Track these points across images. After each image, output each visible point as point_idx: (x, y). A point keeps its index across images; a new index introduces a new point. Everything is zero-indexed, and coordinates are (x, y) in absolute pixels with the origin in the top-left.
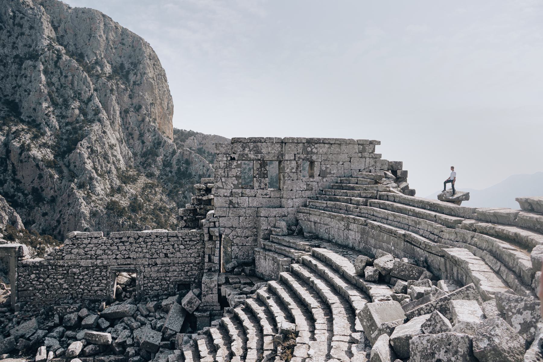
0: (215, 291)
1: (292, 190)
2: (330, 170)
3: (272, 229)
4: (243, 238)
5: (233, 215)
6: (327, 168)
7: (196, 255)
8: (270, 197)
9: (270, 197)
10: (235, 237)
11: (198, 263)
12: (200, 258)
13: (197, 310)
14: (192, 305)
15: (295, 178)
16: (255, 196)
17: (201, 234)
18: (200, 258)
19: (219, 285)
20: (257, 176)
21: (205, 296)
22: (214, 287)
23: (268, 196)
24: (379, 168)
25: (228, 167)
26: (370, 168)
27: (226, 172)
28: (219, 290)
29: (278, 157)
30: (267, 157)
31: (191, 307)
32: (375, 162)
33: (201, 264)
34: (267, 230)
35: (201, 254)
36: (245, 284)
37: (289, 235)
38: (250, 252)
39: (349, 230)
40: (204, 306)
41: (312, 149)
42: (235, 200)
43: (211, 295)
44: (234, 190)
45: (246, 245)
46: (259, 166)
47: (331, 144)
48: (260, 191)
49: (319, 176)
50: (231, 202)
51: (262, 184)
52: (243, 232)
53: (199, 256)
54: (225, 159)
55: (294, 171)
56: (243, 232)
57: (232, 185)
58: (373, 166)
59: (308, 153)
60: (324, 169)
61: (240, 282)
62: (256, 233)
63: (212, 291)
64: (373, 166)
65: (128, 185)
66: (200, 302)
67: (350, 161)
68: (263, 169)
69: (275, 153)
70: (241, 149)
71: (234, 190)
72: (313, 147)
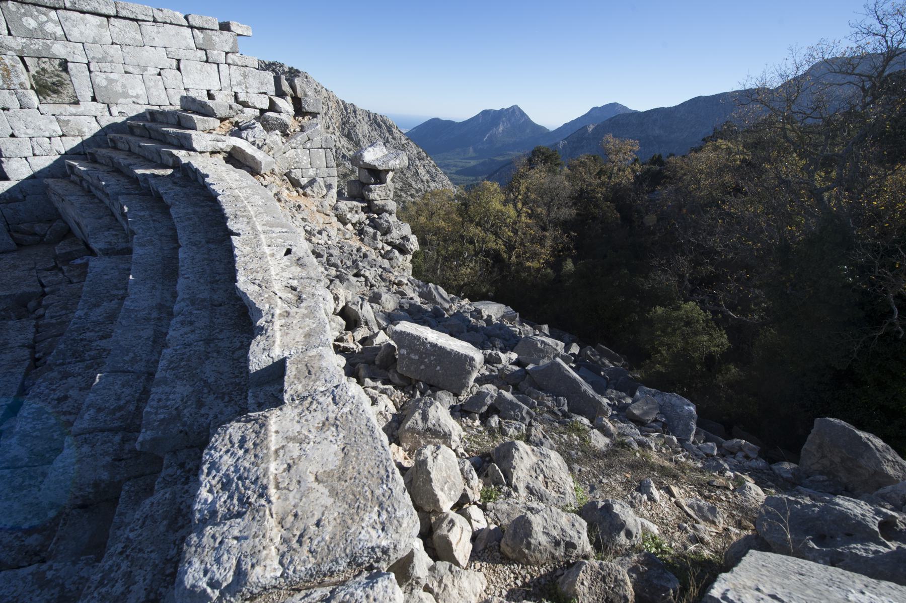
1: (12, 136)
2: (124, 86)
6: (110, 81)
24: (257, 91)
26: (235, 89)
32: (245, 76)
41: (41, 25)
47: (108, 17)
49: (94, 99)
58: (239, 84)
59: (31, 35)
60: (104, 83)
64: (239, 84)
65: (48, 98)
67: (179, 69)
72: (44, 18)
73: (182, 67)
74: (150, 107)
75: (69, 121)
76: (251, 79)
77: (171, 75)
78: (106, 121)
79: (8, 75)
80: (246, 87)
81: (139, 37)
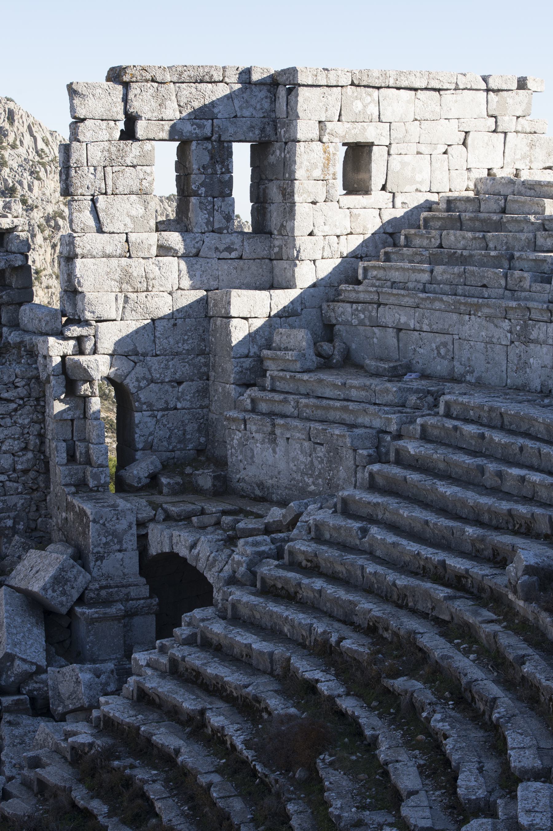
1: (311, 234)
3: (265, 352)
4: (167, 387)
6: (404, 164)
7: (17, 445)
8: (241, 258)
9: (241, 258)
10: (143, 383)
11: (25, 472)
12: (30, 455)
13: (81, 601)
14: (67, 588)
15: (321, 198)
17: (30, 379)
18: (30, 455)
19: (141, 524)
20: (203, 190)
21: (100, 558)
22: (125, 531)
23: (234, 255)
27: (110, 176)
28: (143, 539)
29: (263, 130)
30: (231, 130)
31: (64, 593)
32: (532, 146)
33: (32, 474)
34: (247, 356)
35: (33, 441)
36: (225, 513)
37: (320, 368)
38: (189, 428)
39: (528, 341)
40: (102, 588)
42: (137, 267)
43: (119, 555)
45: (176, 408)
46: (206, 159)
48: (211, 240)
49: (384, 188)
50: (126, 277)
51: (218, 216)
52: (167, 367)
53: (25, 449)
55: (317, 173)
56: (167, 367)
57: (128, 220)
58: (523, 158)
61: (203, 512)
62: (204, 369)
63: (120, 542)
64: (523, 158)
66: (88, 576)
67: (464, 144)
68: (218, 167)
69: (252, 117)
70: (154, 104)
73: (469, 141)
74: (450, 194)
75: (359, 215)
76: (538, 150)
77: (457, 150)
78: (389, 214)
79: (328, 164)
80: (531, 162)
81: (438, 109)
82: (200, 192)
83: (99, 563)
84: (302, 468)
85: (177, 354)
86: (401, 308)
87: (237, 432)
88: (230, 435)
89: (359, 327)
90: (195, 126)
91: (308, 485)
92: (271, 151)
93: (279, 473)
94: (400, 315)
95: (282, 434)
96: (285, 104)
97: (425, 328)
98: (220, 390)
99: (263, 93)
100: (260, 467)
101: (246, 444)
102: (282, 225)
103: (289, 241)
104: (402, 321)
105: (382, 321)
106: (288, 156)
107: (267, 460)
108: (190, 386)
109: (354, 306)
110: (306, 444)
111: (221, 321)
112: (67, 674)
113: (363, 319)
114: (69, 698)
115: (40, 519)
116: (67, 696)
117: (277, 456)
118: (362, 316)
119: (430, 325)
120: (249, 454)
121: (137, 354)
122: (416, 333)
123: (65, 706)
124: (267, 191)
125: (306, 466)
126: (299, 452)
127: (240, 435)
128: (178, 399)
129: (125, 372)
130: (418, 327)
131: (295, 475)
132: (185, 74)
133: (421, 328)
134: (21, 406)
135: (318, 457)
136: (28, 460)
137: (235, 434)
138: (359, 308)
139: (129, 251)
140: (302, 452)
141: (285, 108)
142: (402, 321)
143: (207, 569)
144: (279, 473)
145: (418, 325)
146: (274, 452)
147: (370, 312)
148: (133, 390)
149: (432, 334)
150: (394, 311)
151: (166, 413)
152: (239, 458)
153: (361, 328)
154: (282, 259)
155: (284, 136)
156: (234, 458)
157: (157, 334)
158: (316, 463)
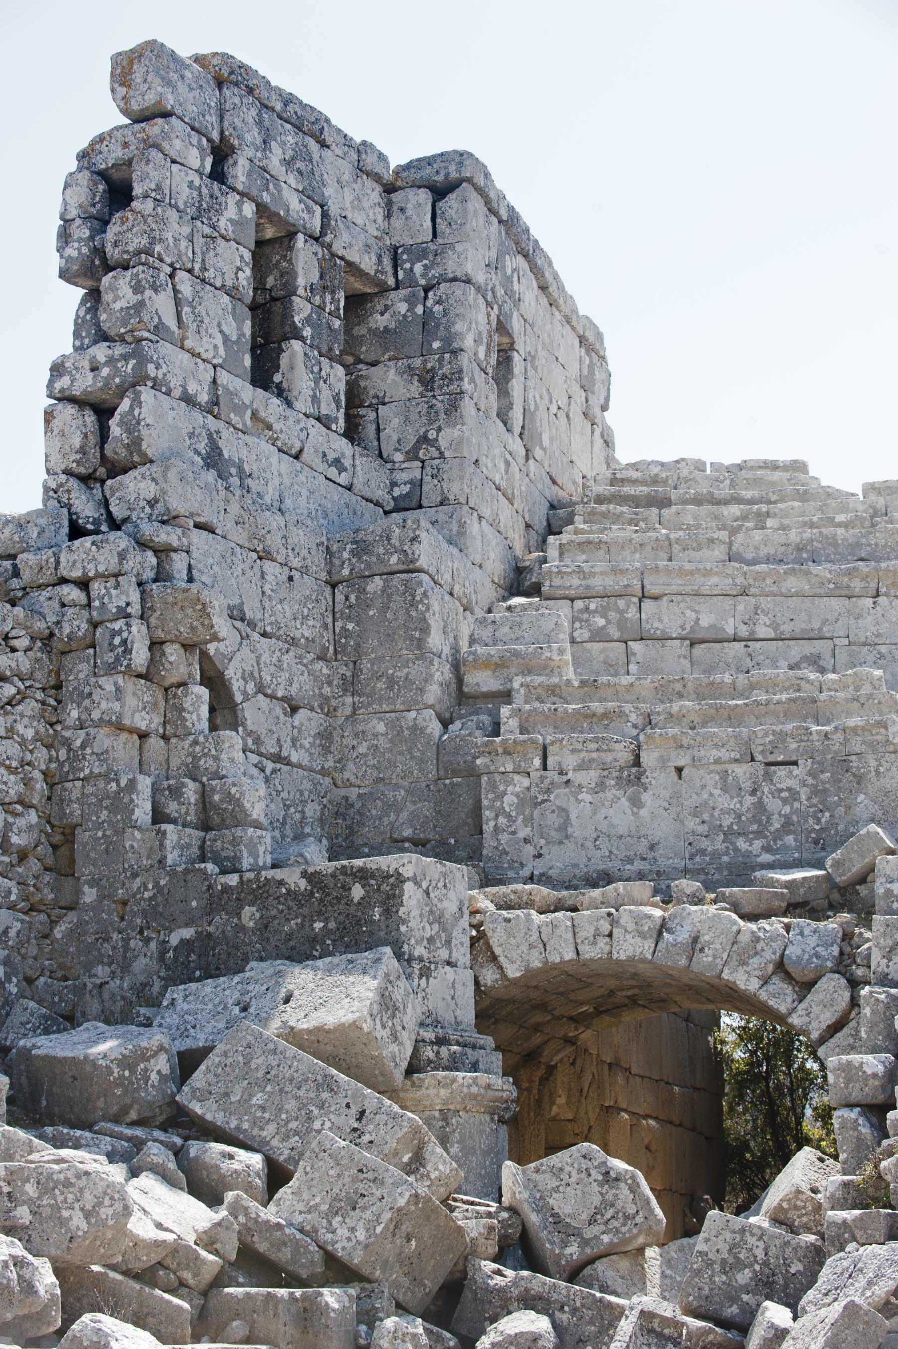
0: (462, 954)
5: (239, 535)
8: (349, 488)
11: (23, 856)
12: (33, 817)
16: (297, 457)
18: (33, 817)
23: (343, 479)
25: (203, 212)
33: (34, 865)
35: (40, 785)
44: (224, 377)
45: (289, 763)
46: (315, 277)
54: (193, 158)
57: (218, 339)
68: (328, 297)
71: (224, 377)
82: (305, 334)
83: (423, 982)
84: (726, 824)
85: (293, 642)
86: (702, 600)
87: (517, 778)
88: (496, 788)
89: (589, 646)
90: (303, 206)
91: (748, 854)
92: (379, 307)
93: (652, 847)
94: (697, 612)
95: (663, 761)
96: (429, 216)
97: (763, 632)
98: (381, 727)
99: (374, 194)
100: (590, 845)
101: (544, 801)
102: (424, 439)
103: (446, 467)
104: (705, 622)
105: (655, 626)
106: (437, 308)
107: (611, 825)
108: (310, 719)
109: (579, 604)
110: (741, 771)
111: (385, 581)
112: (567, 1169)
113: (604, 627)
114: (592, 1221)
115: (42, 980)
116: (584, 1217)
117: (644, 812)
118: (600, 622)
119: (775, 626)
120: (553, 820)
121: (243, 620)
122: (737, 645)
123: (585, 1243)
124: (363, 383)
125: (739, 817)
126: (718, 792)
127: (526, 782)
128: (294, 741)
129: (230, 649)
130: (744, 631)
131: (705, 844)
132: (291, 107)
133: (753, 633)
134: (22, 696)
135: (781, 791)
136: (30, 827)
137: (511, 782)
138: (592, 607)
139: (216, 404)
140: (725, 790)
141: (428, 224)
142: (705, 622)
143: (734, 963)
144: (652, 847)
145: (745, 628)
146: (636, 803)
147: (621, 612)
148: (239, 698)
149: (780, 643)
150: (682, 605)
151: (278, 766)
152: (521, 835)
153: (597, 647)
154: (420, 507)
155: (424, 275)
156: (504, 838)
157: (267, 588)
158: (773, 805)
